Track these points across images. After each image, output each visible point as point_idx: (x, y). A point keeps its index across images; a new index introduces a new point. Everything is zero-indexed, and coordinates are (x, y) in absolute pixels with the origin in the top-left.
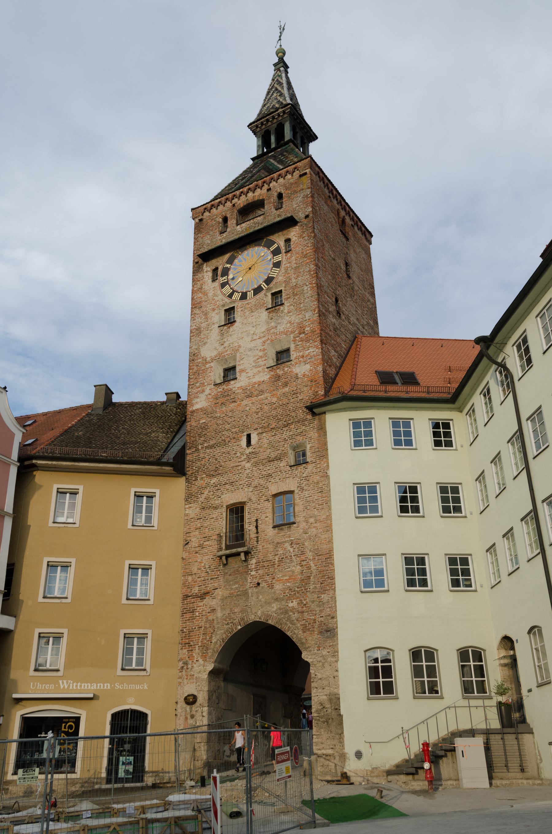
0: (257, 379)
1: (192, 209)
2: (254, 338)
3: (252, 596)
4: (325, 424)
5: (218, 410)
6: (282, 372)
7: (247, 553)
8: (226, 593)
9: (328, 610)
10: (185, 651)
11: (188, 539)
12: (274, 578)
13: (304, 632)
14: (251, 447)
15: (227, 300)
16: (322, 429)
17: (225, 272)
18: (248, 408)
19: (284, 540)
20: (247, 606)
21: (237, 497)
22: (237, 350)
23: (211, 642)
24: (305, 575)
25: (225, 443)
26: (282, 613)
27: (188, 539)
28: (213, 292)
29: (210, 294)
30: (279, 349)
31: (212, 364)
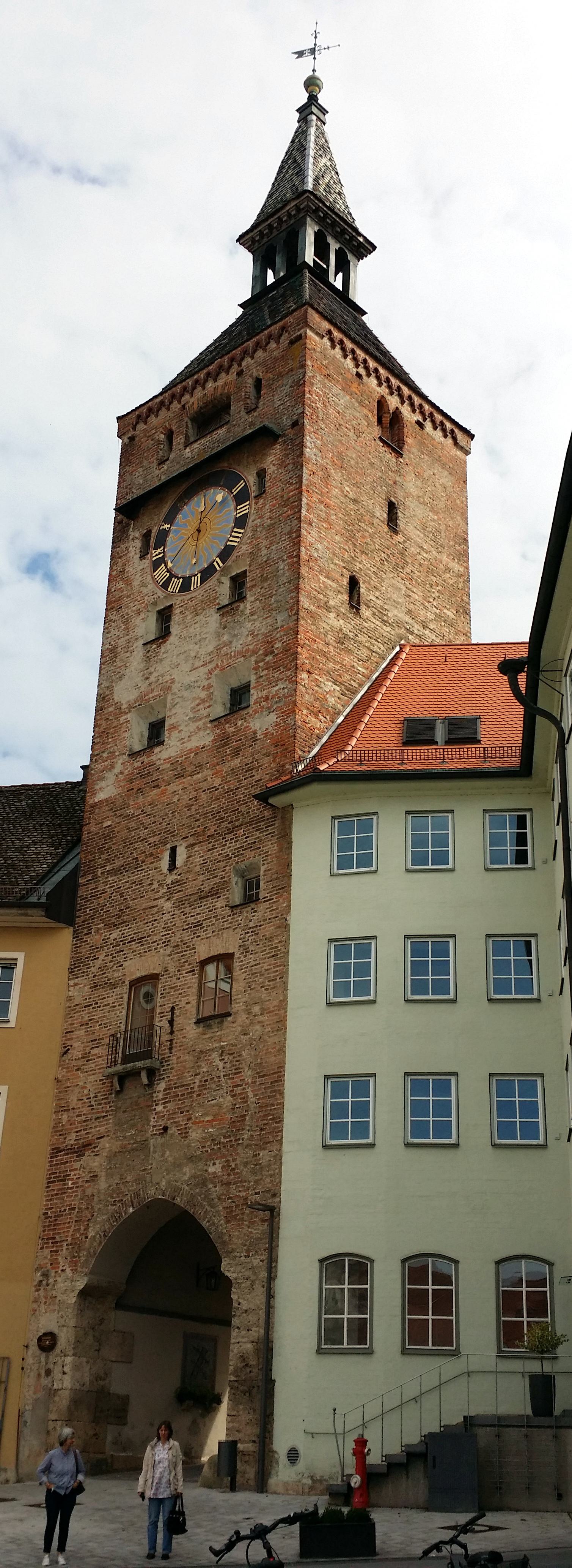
0: (194, 743)
1: (118, 418)
2: (195, 666)
3: (155, 1152)
4: (290, 828)
5: (131, 803)
6: (232, 729)
7: (152, 1073)
8: (116, 1145)
9: (268, 1180)
10: (47, 1252)
11: (69, 1043)
12: (189, 1119)
13: (228, 1222)
14: (175, 872)
15: (160, 593)
16: (285, 839)
18: (175, 799)
19: (211, 1046)
20: (145, 1170)
21: (146, 965)
22: (169, 688)
23: (87, 1238)
24: (238, 1112)
25: (136, 865)
26: (196, 1185)
27: (69, 1043)
28: (140, 579)
29: (136, 583)
30: (235, 684)
31: (129, 716)
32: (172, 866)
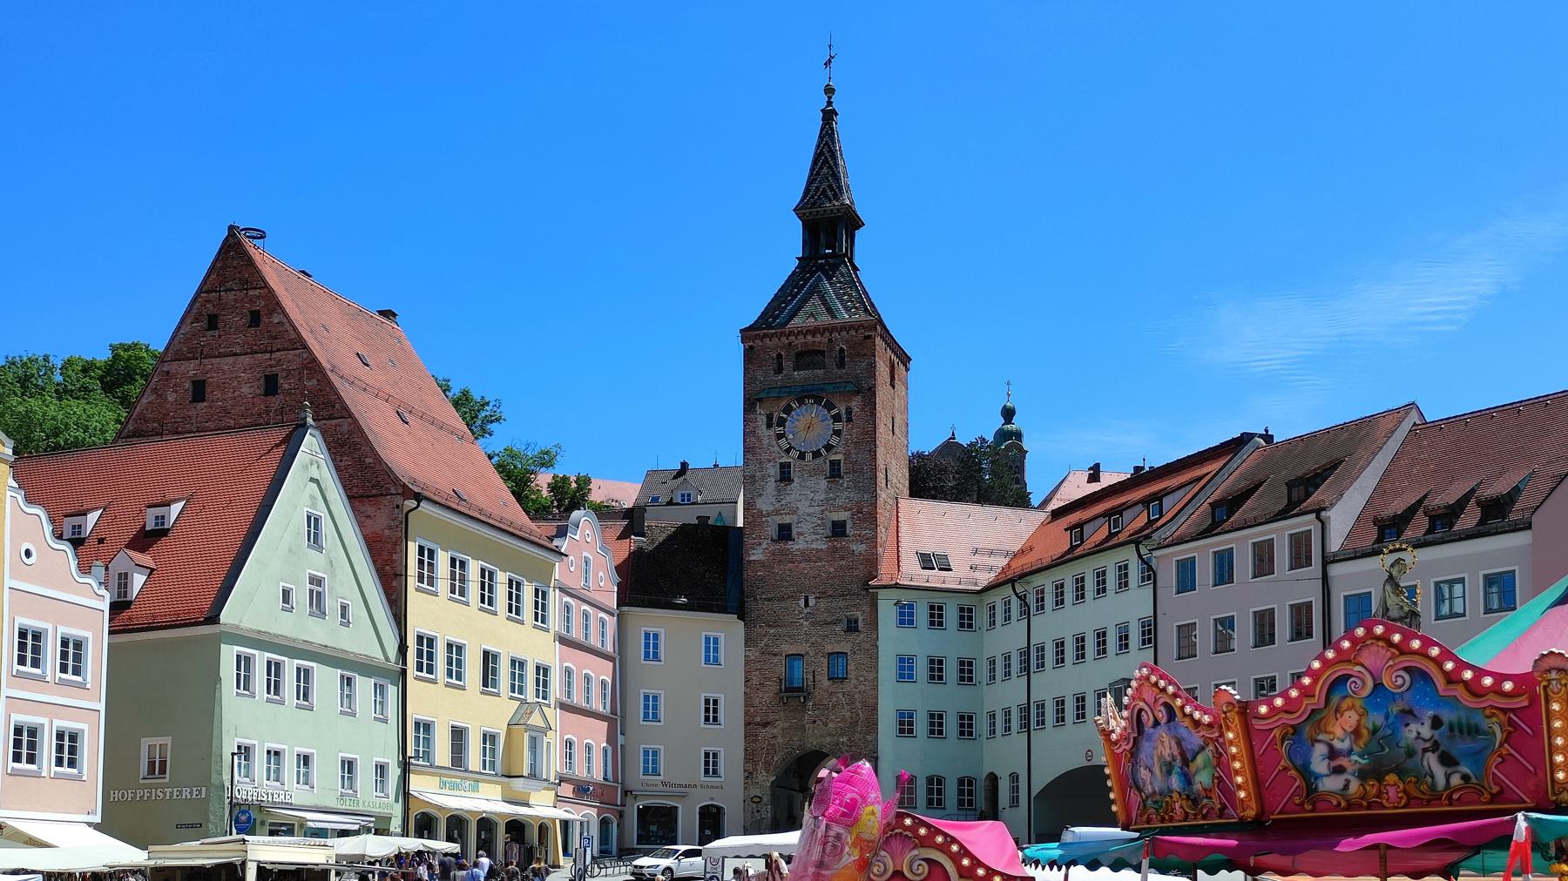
17: (782, 422)
29: (765, 441)
32: (807, 604)
